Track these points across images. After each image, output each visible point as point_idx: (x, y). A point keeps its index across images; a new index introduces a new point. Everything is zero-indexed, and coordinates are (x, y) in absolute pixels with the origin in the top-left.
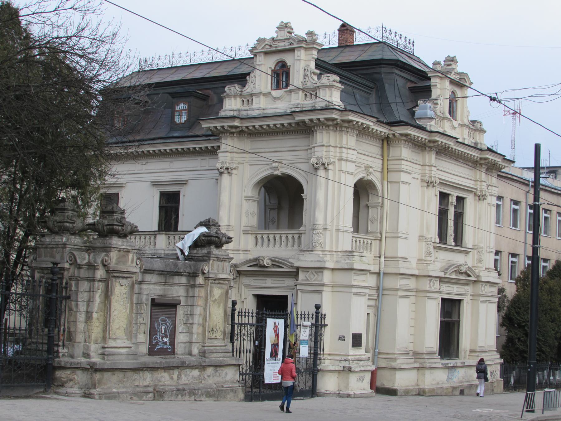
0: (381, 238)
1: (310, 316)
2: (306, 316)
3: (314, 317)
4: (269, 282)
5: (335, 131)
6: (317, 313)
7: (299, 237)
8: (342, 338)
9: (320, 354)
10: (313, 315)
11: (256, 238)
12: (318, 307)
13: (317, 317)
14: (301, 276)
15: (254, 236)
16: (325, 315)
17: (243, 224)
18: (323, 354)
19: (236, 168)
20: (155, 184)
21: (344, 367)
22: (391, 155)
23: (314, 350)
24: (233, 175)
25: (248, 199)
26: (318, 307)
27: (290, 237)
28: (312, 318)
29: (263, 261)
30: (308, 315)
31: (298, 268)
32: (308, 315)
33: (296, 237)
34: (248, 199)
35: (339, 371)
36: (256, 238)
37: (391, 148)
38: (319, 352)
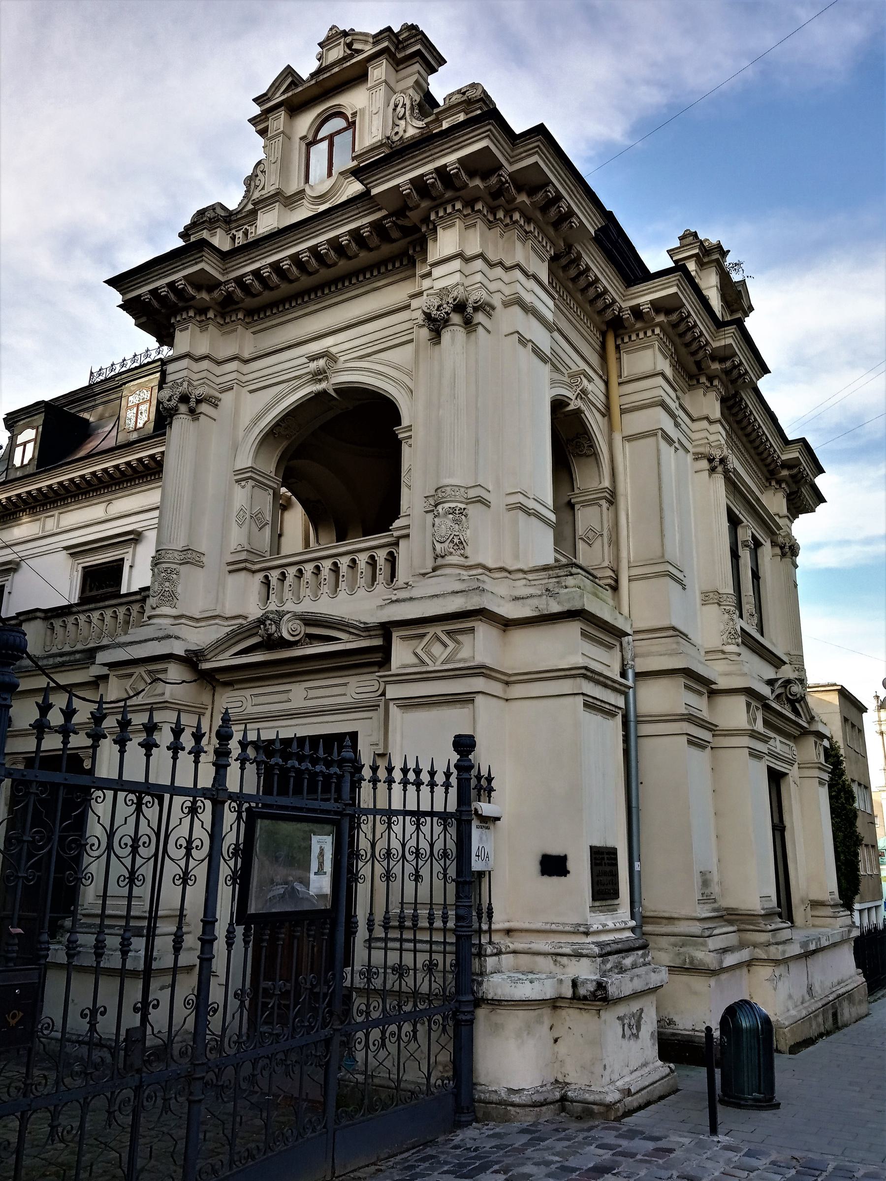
0: (616, 581)
1: (440, 778)
2: (425, 777)
3: (453, 780)
4: (299, 694)
5: (491, 225)
6: (464, 767)
7: (392, 560)
8: (553, 865)
9: (480, 931)
10: (448, 775)
11: (267, 582)
12: (464, 745)
13: (463, 785)
14: (402, 655)
15: (260, 576)
16: (490, 779)
17: (233, 546)
18: (490, 931)
19: (214, 403)
20: (75, 551)
21: (575, 984)
22: (625, 373)
23: (458, 918)
24: (202, 417)
25: (243, 477)
26: (464, 745)
27: (362, 559)
28: (447, 785)
29: (278, 625)
30: (432, 773)
31: (386, 629)
32: (432, 773)
33: (381, 556)
34: (243, 477)
35: (555, 1004)
36: (267, 582)
37: (625, 357)
38: (476, 926)
